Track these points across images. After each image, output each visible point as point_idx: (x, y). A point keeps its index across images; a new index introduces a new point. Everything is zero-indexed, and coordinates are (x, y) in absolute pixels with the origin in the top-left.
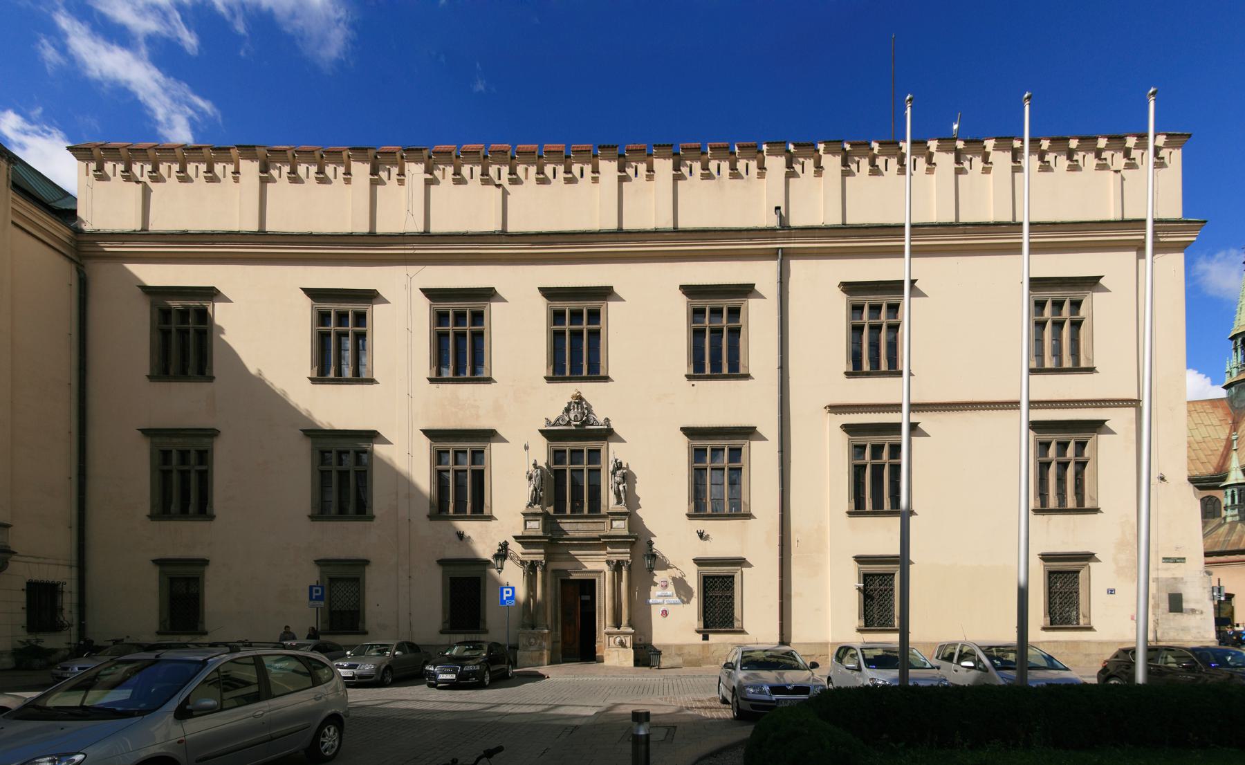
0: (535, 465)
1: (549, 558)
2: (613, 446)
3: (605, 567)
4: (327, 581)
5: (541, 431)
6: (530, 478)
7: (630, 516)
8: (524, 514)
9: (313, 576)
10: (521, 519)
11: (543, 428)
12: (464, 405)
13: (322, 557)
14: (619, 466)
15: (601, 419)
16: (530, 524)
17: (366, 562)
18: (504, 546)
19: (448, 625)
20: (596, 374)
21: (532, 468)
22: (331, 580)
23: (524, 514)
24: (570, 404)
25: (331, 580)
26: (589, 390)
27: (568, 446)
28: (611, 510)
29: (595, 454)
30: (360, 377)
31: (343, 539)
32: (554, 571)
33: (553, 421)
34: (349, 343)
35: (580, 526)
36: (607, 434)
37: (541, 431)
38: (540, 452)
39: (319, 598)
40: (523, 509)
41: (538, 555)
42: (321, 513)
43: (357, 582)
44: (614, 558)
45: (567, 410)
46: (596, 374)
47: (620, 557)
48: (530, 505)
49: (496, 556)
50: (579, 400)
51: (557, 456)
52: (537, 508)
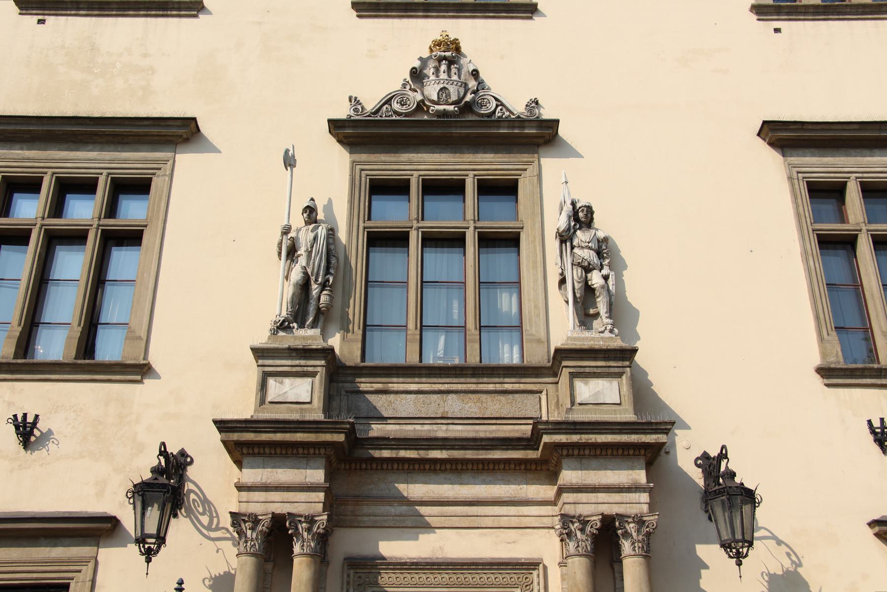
0: (310, 211)
1: (340, 507)
2: (551, 166)
3: (545, 546)
5: (335, 125)
6: (292, 253)
8: (259, 353)
10: (251, 372)
14: (582, 217)
16: (277, 389)
21: (298, 220)
23: (259, 353)
24: (424, 61)
27: (420, 164)
29: (503, 189)
35: (454, 405)
36: (538, 135)
44: (592, 507)
45: (417, 75)
47: (611, 504)
48: (283, 326)
49: (143, 493)
50: (449, 53)
52: (307, 335)
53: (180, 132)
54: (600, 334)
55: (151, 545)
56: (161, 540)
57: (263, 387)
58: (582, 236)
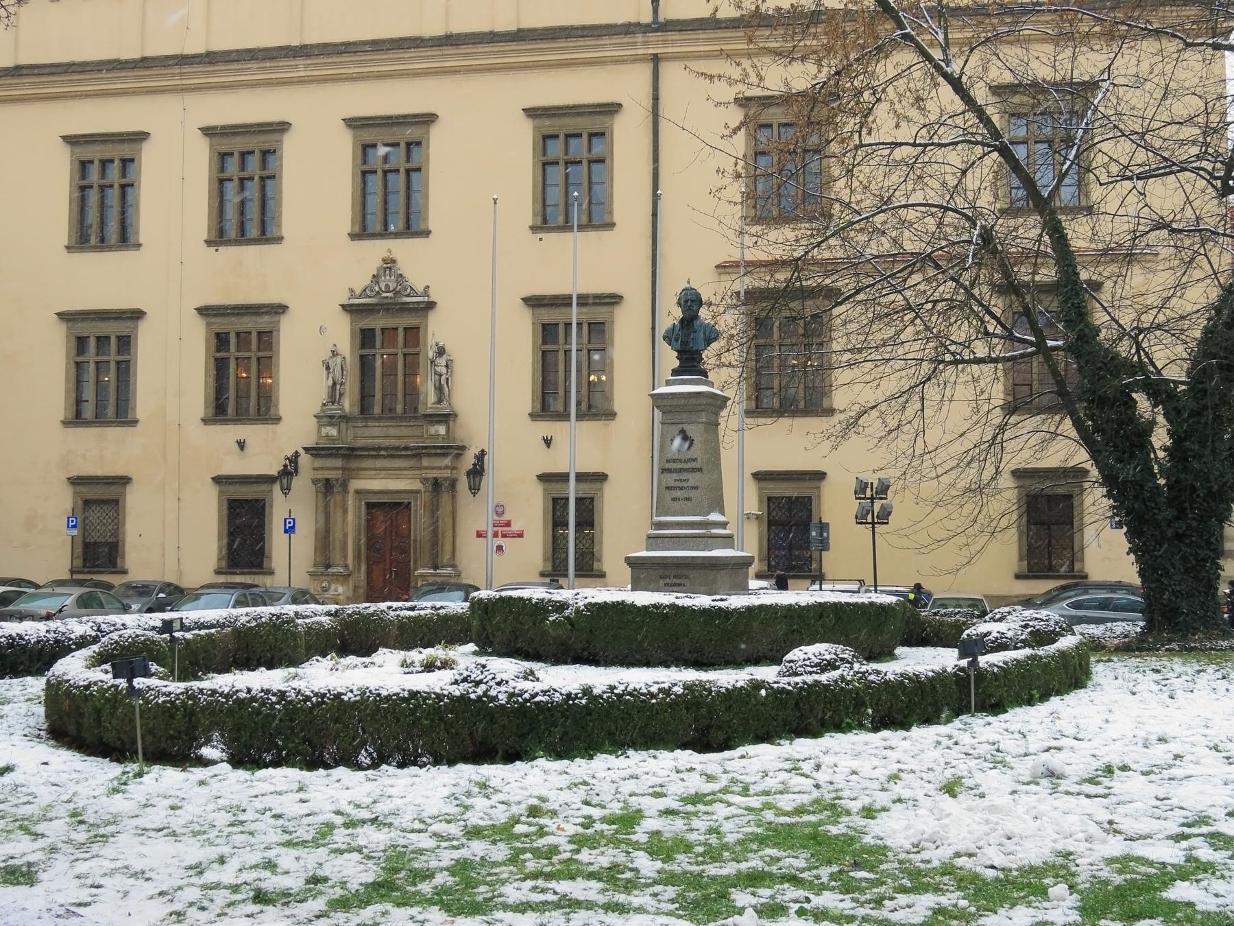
4: (80, 503)
5: (342, 306)
7: (447, 418)
9: (63, 501)
11: (346, 302)
12: (246, 275)
13: (75, 473)
14: (441, 351)
15: (420, 288)
16: (324, 431)
17: (124, 481)
18: (294, 460)
19: (224, 563)
20: (413, 228)
22: (87, 503)
25: (87, 503)
26: (404, 250)
28: (430, 411)
29: (414, 335)
30: (126, 239)
31: (101, 451)
32: (358, 492)
33: (358, 292)
34: (113, 196)
35: (392, 431)
37: (342, 306)
38: (342, 334)
39: (74, 527)
40: (317, 409)
41: (332, 468)
42: (76, 419)
43: (115, 505)
46: (413, 227)
50: (389, 264)
51: (365, 338)
53: (280, 309)
54: (444, 408)
55: (286, 490)
56: (289, 489)
57: (319, 431)
58: (439, 361)
